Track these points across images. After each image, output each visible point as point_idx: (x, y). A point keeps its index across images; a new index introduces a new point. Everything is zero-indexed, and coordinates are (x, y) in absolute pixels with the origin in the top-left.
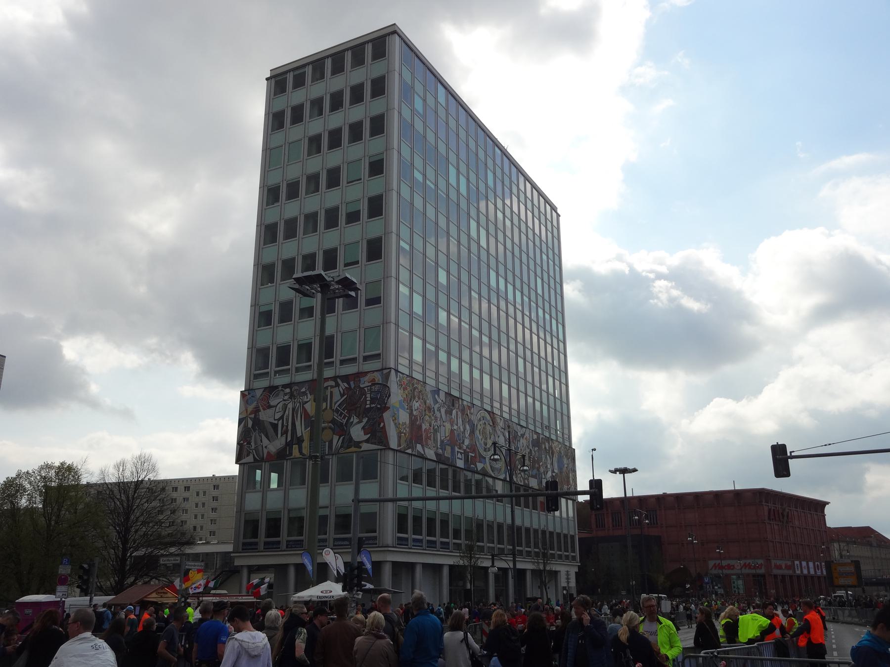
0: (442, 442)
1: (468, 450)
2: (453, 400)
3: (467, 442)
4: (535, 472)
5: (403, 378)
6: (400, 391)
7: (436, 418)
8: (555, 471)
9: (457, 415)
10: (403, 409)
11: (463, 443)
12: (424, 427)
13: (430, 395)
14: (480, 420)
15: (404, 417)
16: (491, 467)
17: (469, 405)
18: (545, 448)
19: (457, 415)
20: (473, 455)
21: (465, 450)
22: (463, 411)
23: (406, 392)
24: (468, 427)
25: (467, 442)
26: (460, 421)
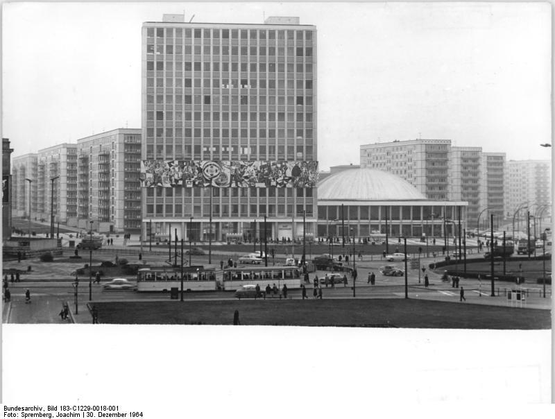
0: (175, 180)
10: (149, 172)
11: (193, 177)
15: (150, 176)
18: (277, 167)
24: (197, 171)
26: (190, 169)
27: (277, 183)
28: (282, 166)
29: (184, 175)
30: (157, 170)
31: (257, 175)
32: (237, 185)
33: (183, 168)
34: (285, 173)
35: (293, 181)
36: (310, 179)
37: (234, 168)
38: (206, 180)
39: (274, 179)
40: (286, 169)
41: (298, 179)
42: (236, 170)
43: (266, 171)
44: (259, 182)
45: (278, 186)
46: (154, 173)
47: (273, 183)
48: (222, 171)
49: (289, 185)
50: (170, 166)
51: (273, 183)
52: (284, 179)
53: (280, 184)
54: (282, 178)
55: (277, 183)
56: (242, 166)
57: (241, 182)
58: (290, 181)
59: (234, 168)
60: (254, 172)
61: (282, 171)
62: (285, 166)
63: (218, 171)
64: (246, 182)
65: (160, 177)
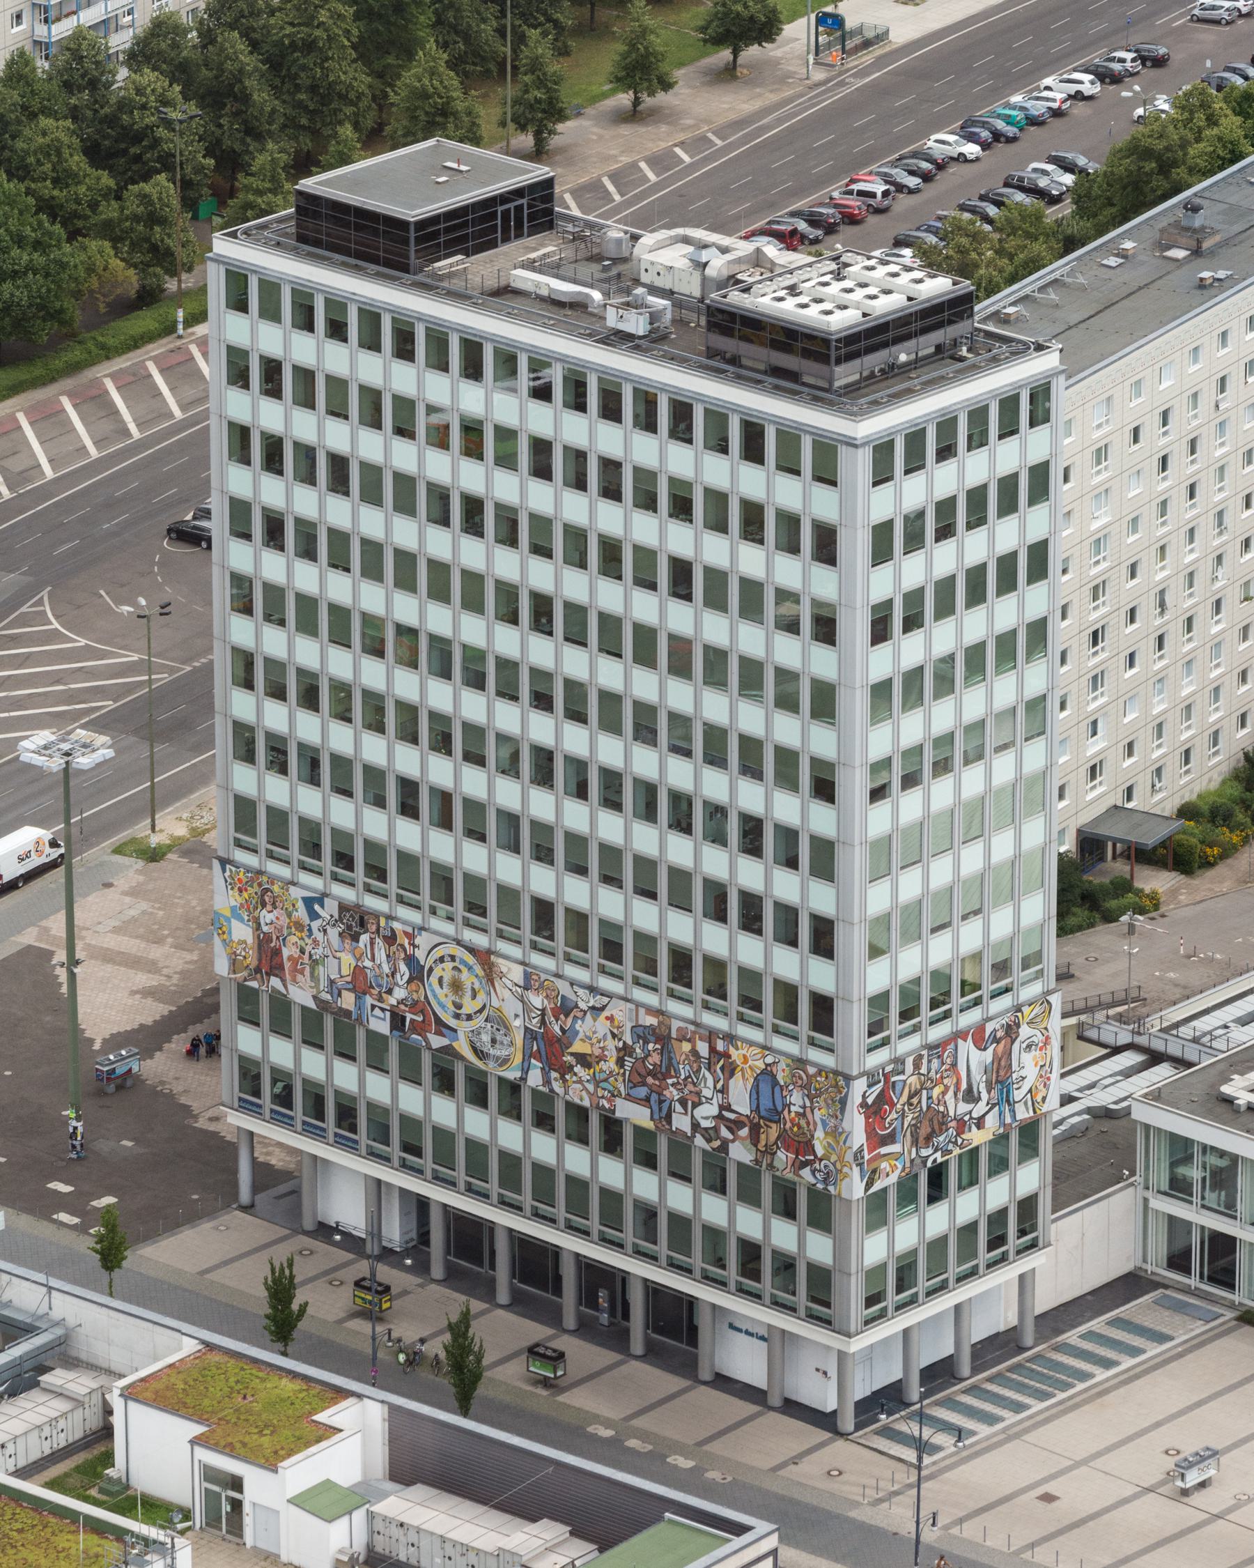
0: (332, 982)
1: (402, 1007)
2: (362, 919)
3: (399, 993)
4: (642, 1092)
5: (238, 873)
6: (230, 892)
7: (315, 941)
8: (734, 1107)
9: (372, 943)
11: (390, 992)
12: (286, 952)
13: (300, 904)
14: (442, 960)
15: (242, 932)
16: (475, 1050)
17: (410, 930)
18: (695, 1052)
19: (372, 943)
20: (420, 1019)
21: (392, 1006)
22: (391, 939)
23: (245, 895)
24: (403, 967)
25: (399, 993)
26: (381, 955)
27: (695, 1126)
28: (712, 1050)
29: (358, 971)
30: (266, 916)
31: (620, 1062)
32: (547, 1082)
33: (355, 938)
34: (724, 1091)
35: (754, 1138)
36: (820, 1151)
37: (537, 1001)
38: (439, 1022)
39: (683, 1102)
40: (730, 1070)
41: (774, 1131)
42: (543, 1010)
43: (655, 1058)
44: (629, 1097)
45: (699, 1141)
46: (258, 927)
47: (681, 1122)
48: (495, 1003)
49: (740, 1153)
50: (314, 916)
51: (681, 1122)
52: (719, 1117)
53: (709, 1135)
54: (713, 1110)
55: (695, 1126)
56: (565, 1008)
57: (565, 1070)
58: (744, 1132)
59: (537, 1001)
60: (611, 1044)
61: (716, 1082)
62: (727, 1055)
63: (482, 997)
64: (580, 1081)
65: (277, 952)
